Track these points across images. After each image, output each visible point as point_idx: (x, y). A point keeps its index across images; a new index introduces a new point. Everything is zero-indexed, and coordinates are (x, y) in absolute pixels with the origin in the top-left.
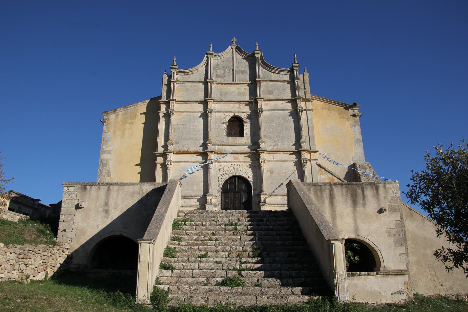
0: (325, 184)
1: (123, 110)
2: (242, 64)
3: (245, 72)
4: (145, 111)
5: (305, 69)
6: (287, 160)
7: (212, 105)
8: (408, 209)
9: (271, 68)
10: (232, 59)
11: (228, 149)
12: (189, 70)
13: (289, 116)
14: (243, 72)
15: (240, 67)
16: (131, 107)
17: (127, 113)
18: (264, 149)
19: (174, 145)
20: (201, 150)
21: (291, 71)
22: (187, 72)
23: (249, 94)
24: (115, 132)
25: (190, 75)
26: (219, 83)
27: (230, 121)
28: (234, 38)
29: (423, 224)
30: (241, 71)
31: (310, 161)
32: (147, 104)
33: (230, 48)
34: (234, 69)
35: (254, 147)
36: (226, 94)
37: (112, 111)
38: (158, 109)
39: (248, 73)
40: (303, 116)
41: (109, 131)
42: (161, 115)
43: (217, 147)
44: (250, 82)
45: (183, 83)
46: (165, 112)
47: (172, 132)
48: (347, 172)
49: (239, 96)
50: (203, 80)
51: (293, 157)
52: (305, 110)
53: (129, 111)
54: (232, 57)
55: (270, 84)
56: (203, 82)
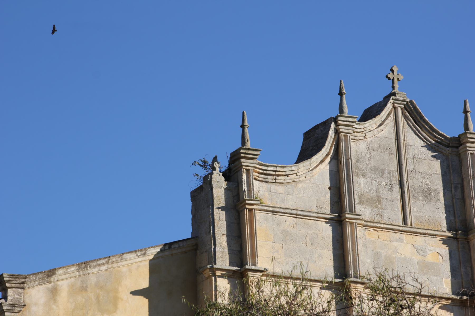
1: (73, 275)
2: (422, 168)
3: (433, 194)
10: (394, 145)
12: (290, 169)
15: (419, 176)
16: (100, 265)
17: (86, 287)
22: (283, 173)
23: (450, 274)
25: (289, 186)
26: (369, 224)
30: (424, 192)
37: (40, 276)
39: (443, 202)
44: (450, 234)
45: (273, 212)
49: (424, 274)
54: (393, 136)
56: (329, 216)
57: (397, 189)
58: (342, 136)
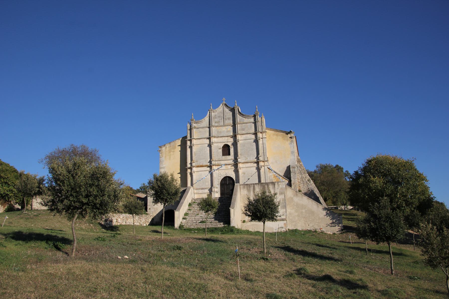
0: (251, 184)
3: (230, 118)
4: (180, 144)
5: (262, 114)
6: (252, 167)
7: (213, 140)
8: (295, 192)
11: (222, 162)
13: (253, 142)
14: (229, 119)
18: (240, 162)
19: (195, 163)
20: (209, 164)
21: (255, 116)
24: (166, 157)
27: (223, 147)
28: (224, 98)
29: (302, 198)
31: (264, 166)
32: (181, 140)
33: (221, 105)
34: (224, 118)
35: (235, 161)
36: (220, 132)
38: (186, 143)
40: (260, 142)
42: (188, 147)
43: (217, 162)
46: (190, 145)
47: (194, 156)
48: (286, 170)
50: (208, 126)
51: (255, 165)
52: (262, 138)
53: (172, 145)
54: (223, 110)
55: (243, 124)
58: (211, 113)
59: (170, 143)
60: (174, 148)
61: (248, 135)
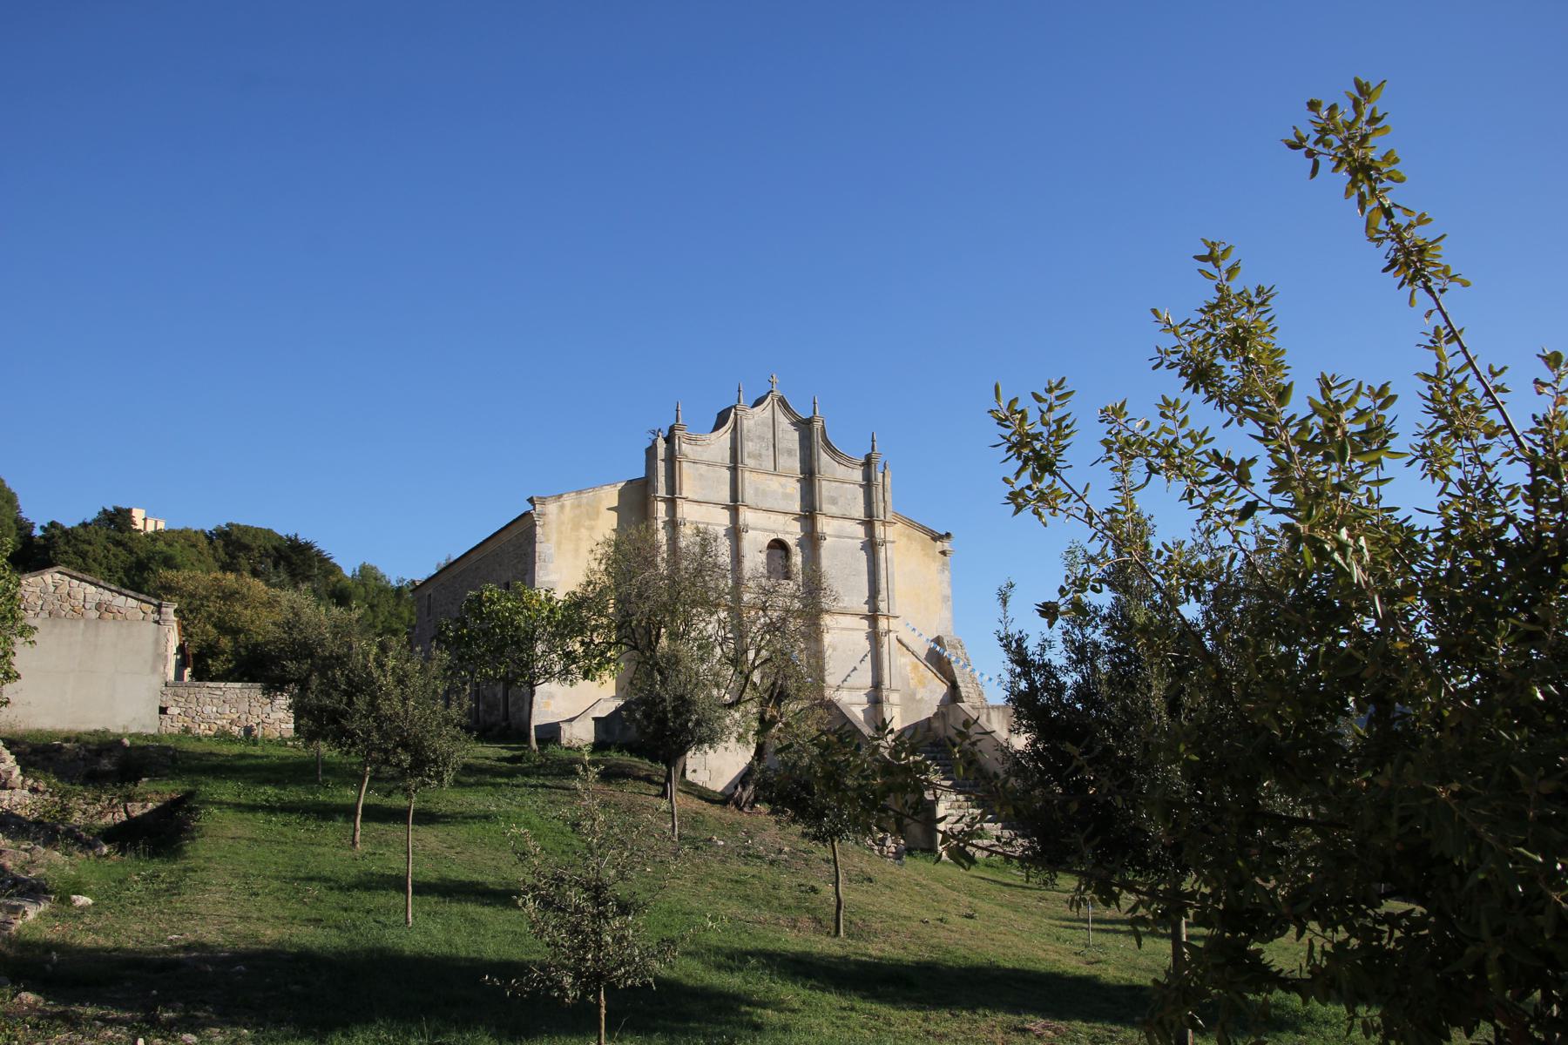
7: (746, 516)
9: (836, 454)
14: (790, 452)
24: (559, 544)
41: (548, 540)
51: (865, 623)
55: (834, 484)
57: (772, 449)
59: (579, 492)
60: (594, 514)
61: (847, 523)
